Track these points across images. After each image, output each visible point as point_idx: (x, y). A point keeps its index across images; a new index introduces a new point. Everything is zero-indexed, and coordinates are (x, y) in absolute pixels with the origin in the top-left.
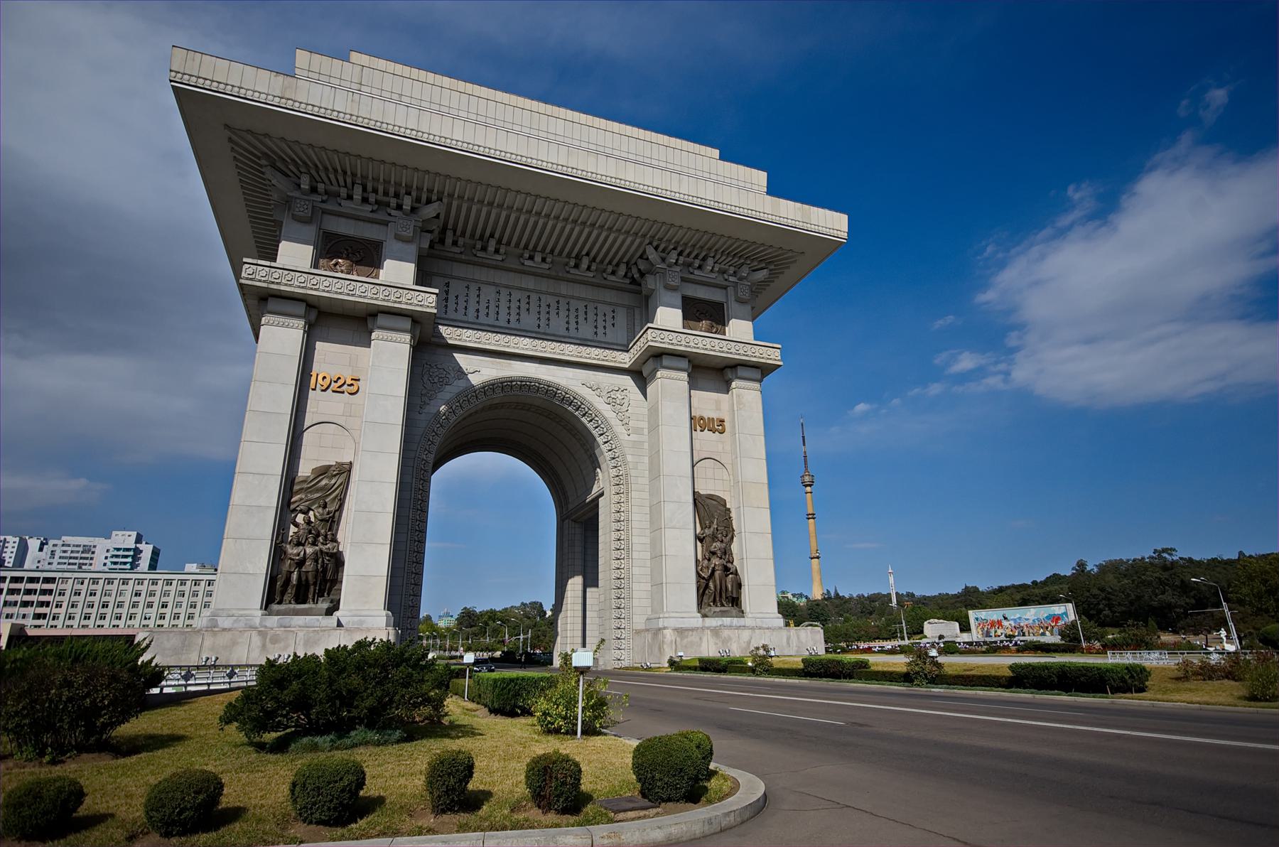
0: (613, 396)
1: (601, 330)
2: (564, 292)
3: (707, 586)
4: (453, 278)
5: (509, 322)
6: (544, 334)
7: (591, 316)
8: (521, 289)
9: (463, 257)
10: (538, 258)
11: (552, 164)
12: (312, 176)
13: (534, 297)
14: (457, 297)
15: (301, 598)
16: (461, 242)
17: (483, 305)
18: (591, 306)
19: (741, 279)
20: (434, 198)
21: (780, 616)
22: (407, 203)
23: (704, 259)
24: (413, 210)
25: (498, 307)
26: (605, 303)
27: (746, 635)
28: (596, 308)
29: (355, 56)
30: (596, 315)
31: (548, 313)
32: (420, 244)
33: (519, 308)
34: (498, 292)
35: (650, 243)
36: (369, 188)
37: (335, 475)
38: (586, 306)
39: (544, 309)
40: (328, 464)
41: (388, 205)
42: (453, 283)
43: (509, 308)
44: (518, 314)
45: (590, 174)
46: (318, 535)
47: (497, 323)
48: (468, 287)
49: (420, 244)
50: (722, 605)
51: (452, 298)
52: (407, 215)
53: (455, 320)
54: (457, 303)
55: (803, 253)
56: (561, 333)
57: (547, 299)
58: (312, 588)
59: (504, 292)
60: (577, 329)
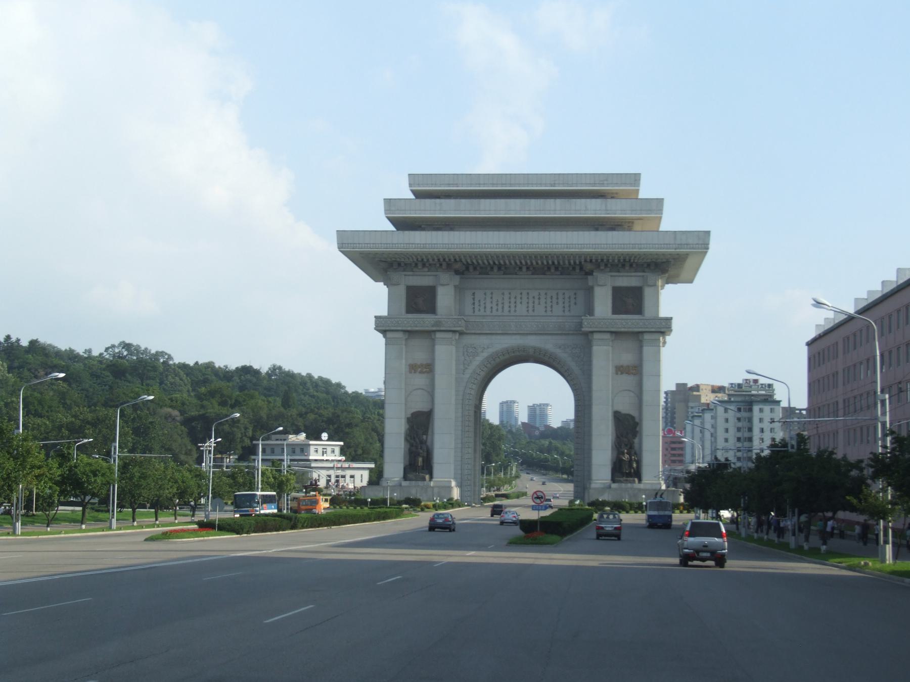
1: (567, 309)
5: (510, 311)
13: (525, 292)
14: (479, 301)
25: (503, 303)
33: (515, 302)
34: (503, 294)
38: (557, 294)
43: (510, 302)
44: (515, 306)
48: (485, 294)
54: (480, 305)
60: (552, 311)
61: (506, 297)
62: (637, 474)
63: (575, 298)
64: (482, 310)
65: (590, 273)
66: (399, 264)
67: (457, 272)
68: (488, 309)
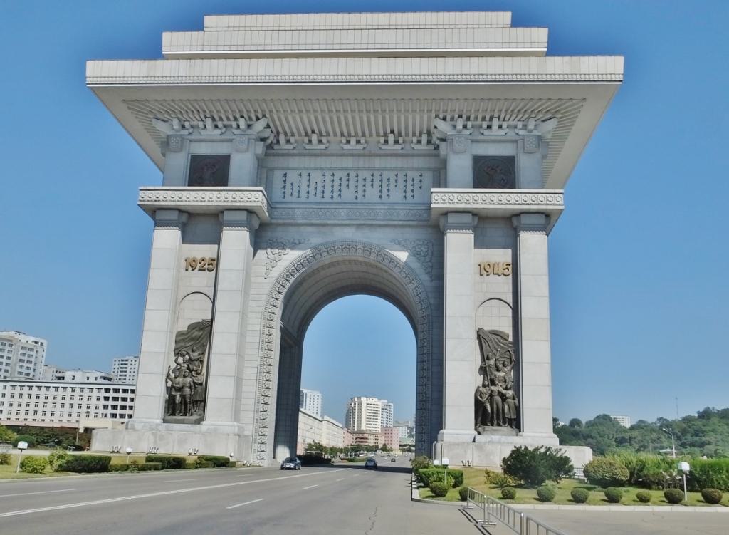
0: (418, 250)
1: (409, 194)
2: (377, 166)
3: (485, 408)
4: (290, 169)
5: (332, 197)
6: (362, 203)
9: (295, 152)
10: (353, 141)
11: (334, 76)
12: (179, 120)
13: (353, 174)
14: (292, 184)
16: (292, 140)
17: (312, 186)
18: (401, 175)
19: (531, 131)
20: (260, 116)
21: (555, 435)
22: (242, 123)
23: (491, 118)
24: (249, 126)
25: (324, 187)
26: (412, 169)
28: (406, 175)
29: (209, 21)
30: (406, 181)
31: (364, 185)
32: (255, 150)
33: (340, 185)
35: (437, 116)
36: (217, 118)
37: (202, 329)
38: (397, 175)
39: (361, 183)
40: (197, 321)
41: (231, 126)
42: (289, 173)
44: (340, 190)
45: (364, 77)
46: (191, 371)
47: (323, 200)
49: (255, 150)
50: (499, 425)
51: (288, 185)
52: (245, 131)
53: (292, 203)
54: (292, 189)
55: (585, 99)
56: (375, 201)
57: (363, 174)
58: (188, 405)
59: (329, 174)
60: (389, 195)
61: (328, 178)
62: (516, 423)
63: (421, 181)
64: (296, 194)
68: (303, 194)
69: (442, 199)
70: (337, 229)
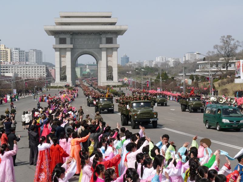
1: (96, 42)
7: (94, 41)
8: (84, 38)
13: (86, 39)
15: (63, 80)
27: (111, 83)
59: (82, 39)
61: (82, 40)
62: (112, 79)
65: (101, 34)
66: (58, 33)
67: (71, 35)
68: (78, 43)
69: (101, 46)
70: (84, 49)
